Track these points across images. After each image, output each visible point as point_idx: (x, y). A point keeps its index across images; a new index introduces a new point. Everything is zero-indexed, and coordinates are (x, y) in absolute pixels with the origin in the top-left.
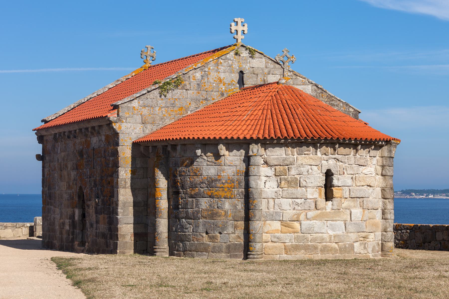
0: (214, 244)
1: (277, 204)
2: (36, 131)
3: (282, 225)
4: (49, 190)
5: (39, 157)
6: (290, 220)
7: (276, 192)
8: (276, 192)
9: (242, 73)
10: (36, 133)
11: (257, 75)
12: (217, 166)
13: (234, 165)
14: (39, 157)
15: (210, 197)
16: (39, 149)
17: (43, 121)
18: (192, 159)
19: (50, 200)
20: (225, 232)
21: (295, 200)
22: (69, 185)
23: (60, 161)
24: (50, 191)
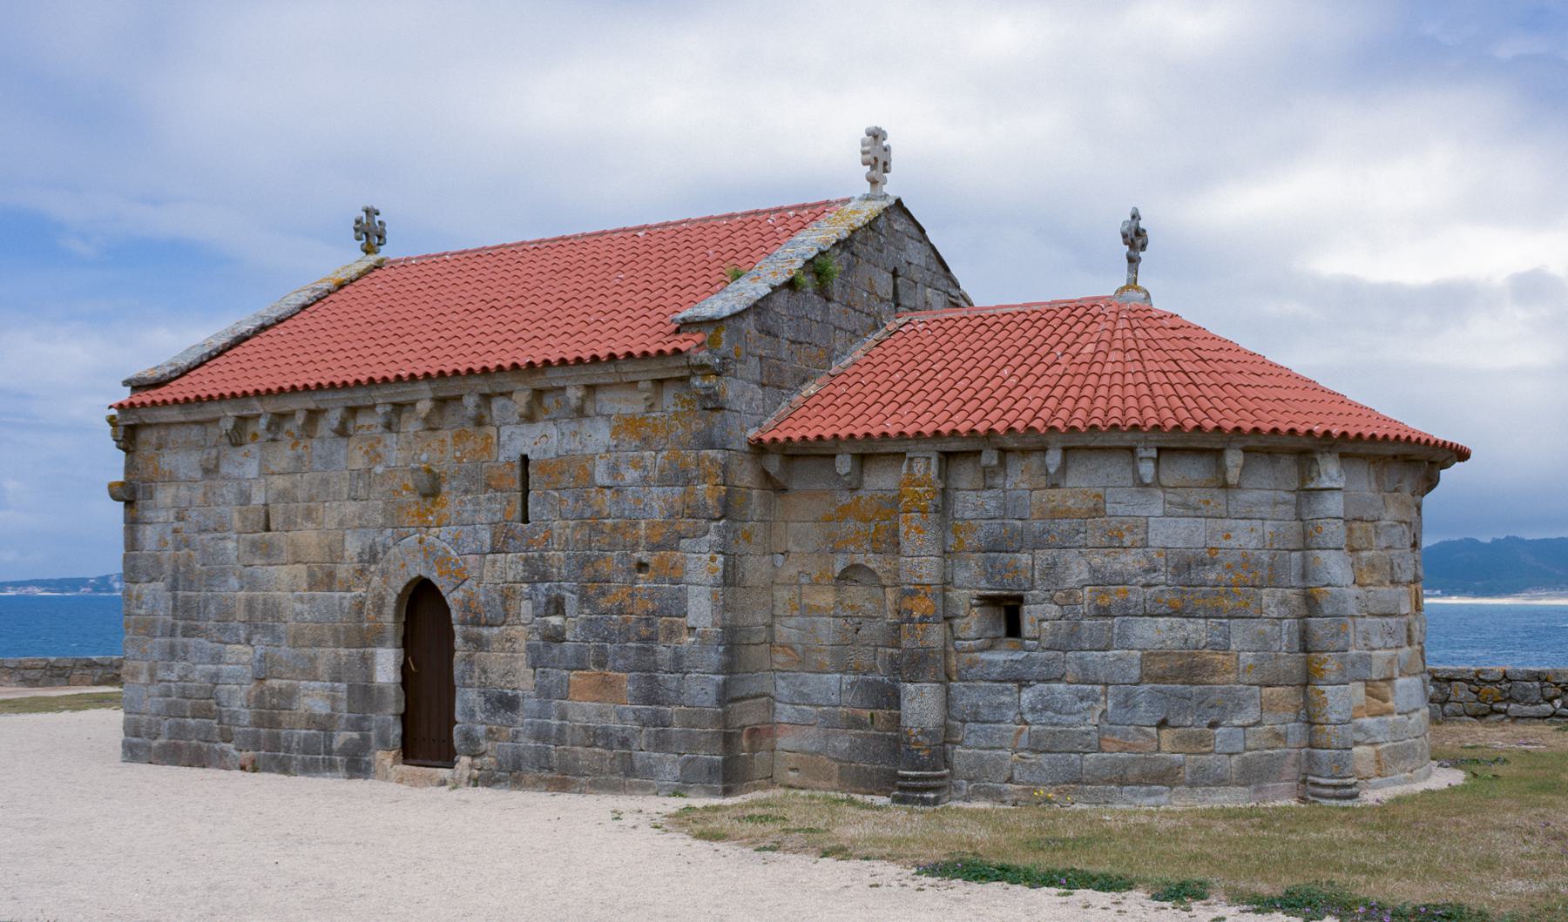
0: (1195, 760)
1: (1361, 632)
2: (114, 412)
3: (1368, 693)
4: (174, 588)
5: (116, 492)
6: (1382, 676)
7: (1357, 598)
8: (1357, 598)
9: (895, 274)
10: (111, 420)
11: (916, 283)
12: (1203, 520)
13: (1258, 515)
14: (116, 492)
15: (1177, 613)
16: (114, 465)
17: (126, 383)
18: (1098, 496)
19: (180, 623)
20: (1236, 722)
21: (1388, 620)
22: (331, 576)
23: (258, 499)
24: (180, 594)
